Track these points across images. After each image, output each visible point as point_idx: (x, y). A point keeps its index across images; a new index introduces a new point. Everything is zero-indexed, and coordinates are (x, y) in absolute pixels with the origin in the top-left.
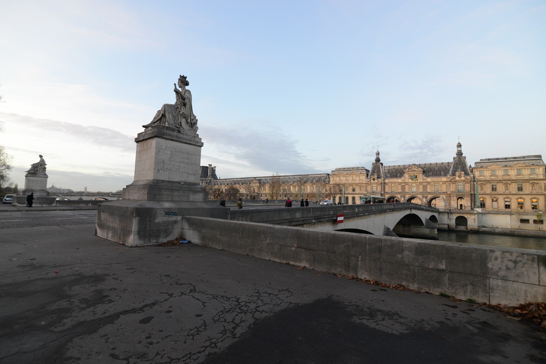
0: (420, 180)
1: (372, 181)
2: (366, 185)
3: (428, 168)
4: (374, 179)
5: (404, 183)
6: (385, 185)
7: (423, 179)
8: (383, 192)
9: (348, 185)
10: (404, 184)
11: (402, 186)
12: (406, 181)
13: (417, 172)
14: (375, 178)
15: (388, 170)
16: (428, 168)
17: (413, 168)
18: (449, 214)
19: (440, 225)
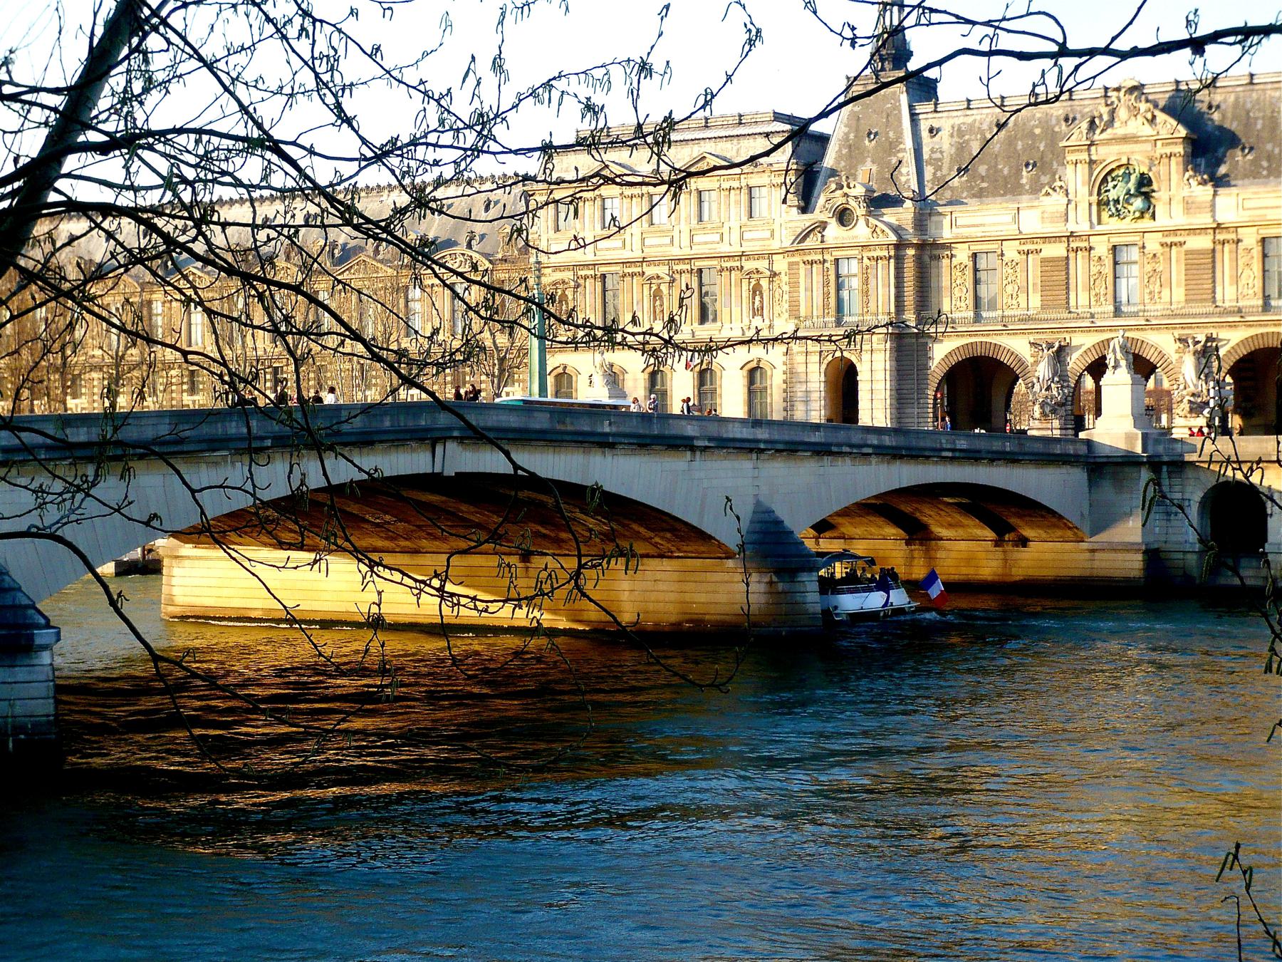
0: (1169, 213)
1: (834, 232)
2: (790, 264)
3: (1229, 115)
4: (843, 216)
5: (1057, 238)
6: (926, 258)
7: (1189, 205)
8: (910, 317)
9: (662, 270)
10: (1058, 250)
11: (1045, 261)
12: (1072, 226)
13: (1148, 147)
14: (853, 203)
15: (960, 133)
16: (1229, 115)
17: (1122, 113)
18: (1165, 468)
19: (1098, 555)
